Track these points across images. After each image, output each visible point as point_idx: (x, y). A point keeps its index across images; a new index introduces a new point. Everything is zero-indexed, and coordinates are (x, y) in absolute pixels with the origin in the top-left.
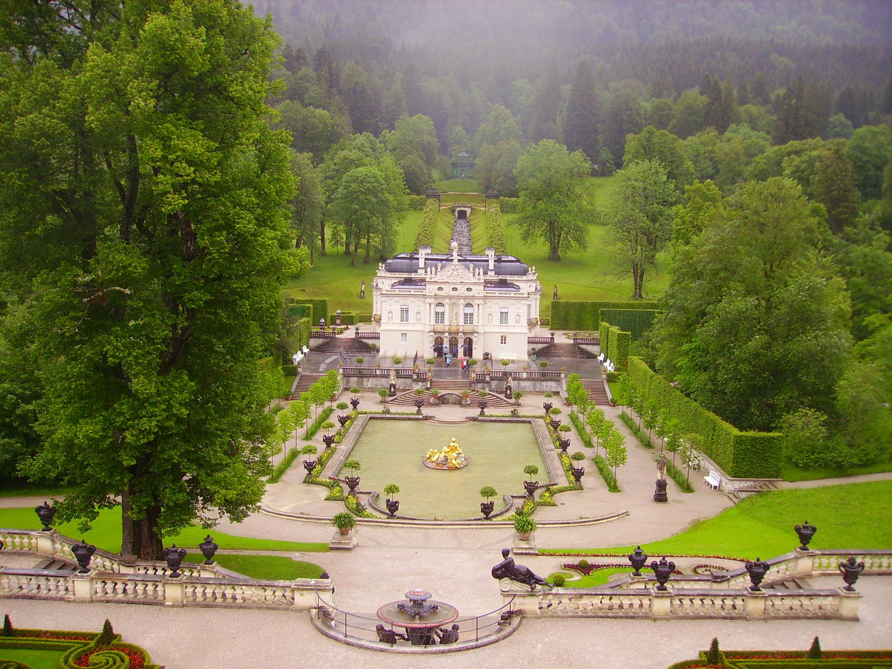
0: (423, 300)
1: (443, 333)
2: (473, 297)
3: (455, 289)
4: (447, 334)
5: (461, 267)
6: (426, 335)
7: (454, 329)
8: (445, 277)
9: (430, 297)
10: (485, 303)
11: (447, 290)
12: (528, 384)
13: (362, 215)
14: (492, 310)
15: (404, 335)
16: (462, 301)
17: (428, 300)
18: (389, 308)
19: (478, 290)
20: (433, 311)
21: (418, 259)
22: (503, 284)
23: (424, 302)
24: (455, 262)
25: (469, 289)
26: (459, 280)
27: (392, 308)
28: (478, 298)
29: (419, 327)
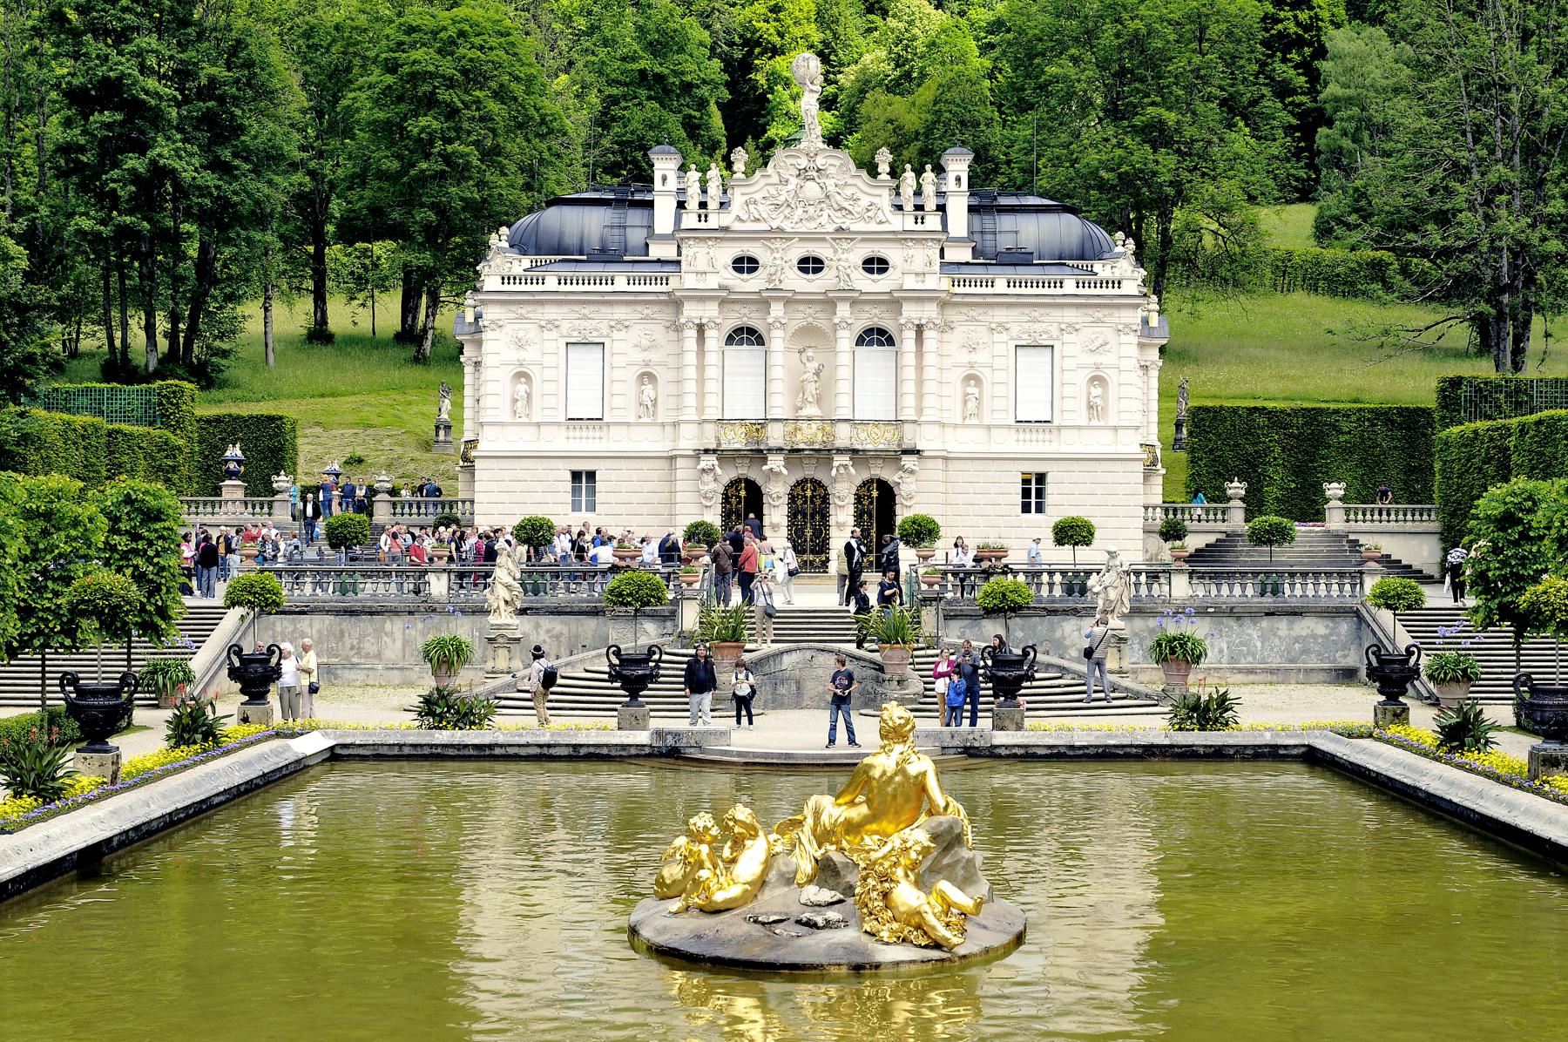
0: (666, 314)
1: (759, 455)
2: (893, 302)
3: (810, 265)
4: (776, 462)
5: (838, 165)
6: (684, 469)
7: (808, 436)
8: (764, 210)
9: (701, 297)
10: (947, 327)
11: (779, 265)
12: (1199, 629)
13: (447, 158)
14: (981, 357)
15: (583, 479)
16: (843, 310)
17: (691, 311)
18: (513, 355)
19: (914, 267)
20: (712, 358)
21: (650, 205)
22: (1017, 259)
23: (678, 329)
24: (813, 139)
25: (876, 265)
26: (827, 221)
27: (530, 355)
28: (921, 298)
29: (652, 441)
